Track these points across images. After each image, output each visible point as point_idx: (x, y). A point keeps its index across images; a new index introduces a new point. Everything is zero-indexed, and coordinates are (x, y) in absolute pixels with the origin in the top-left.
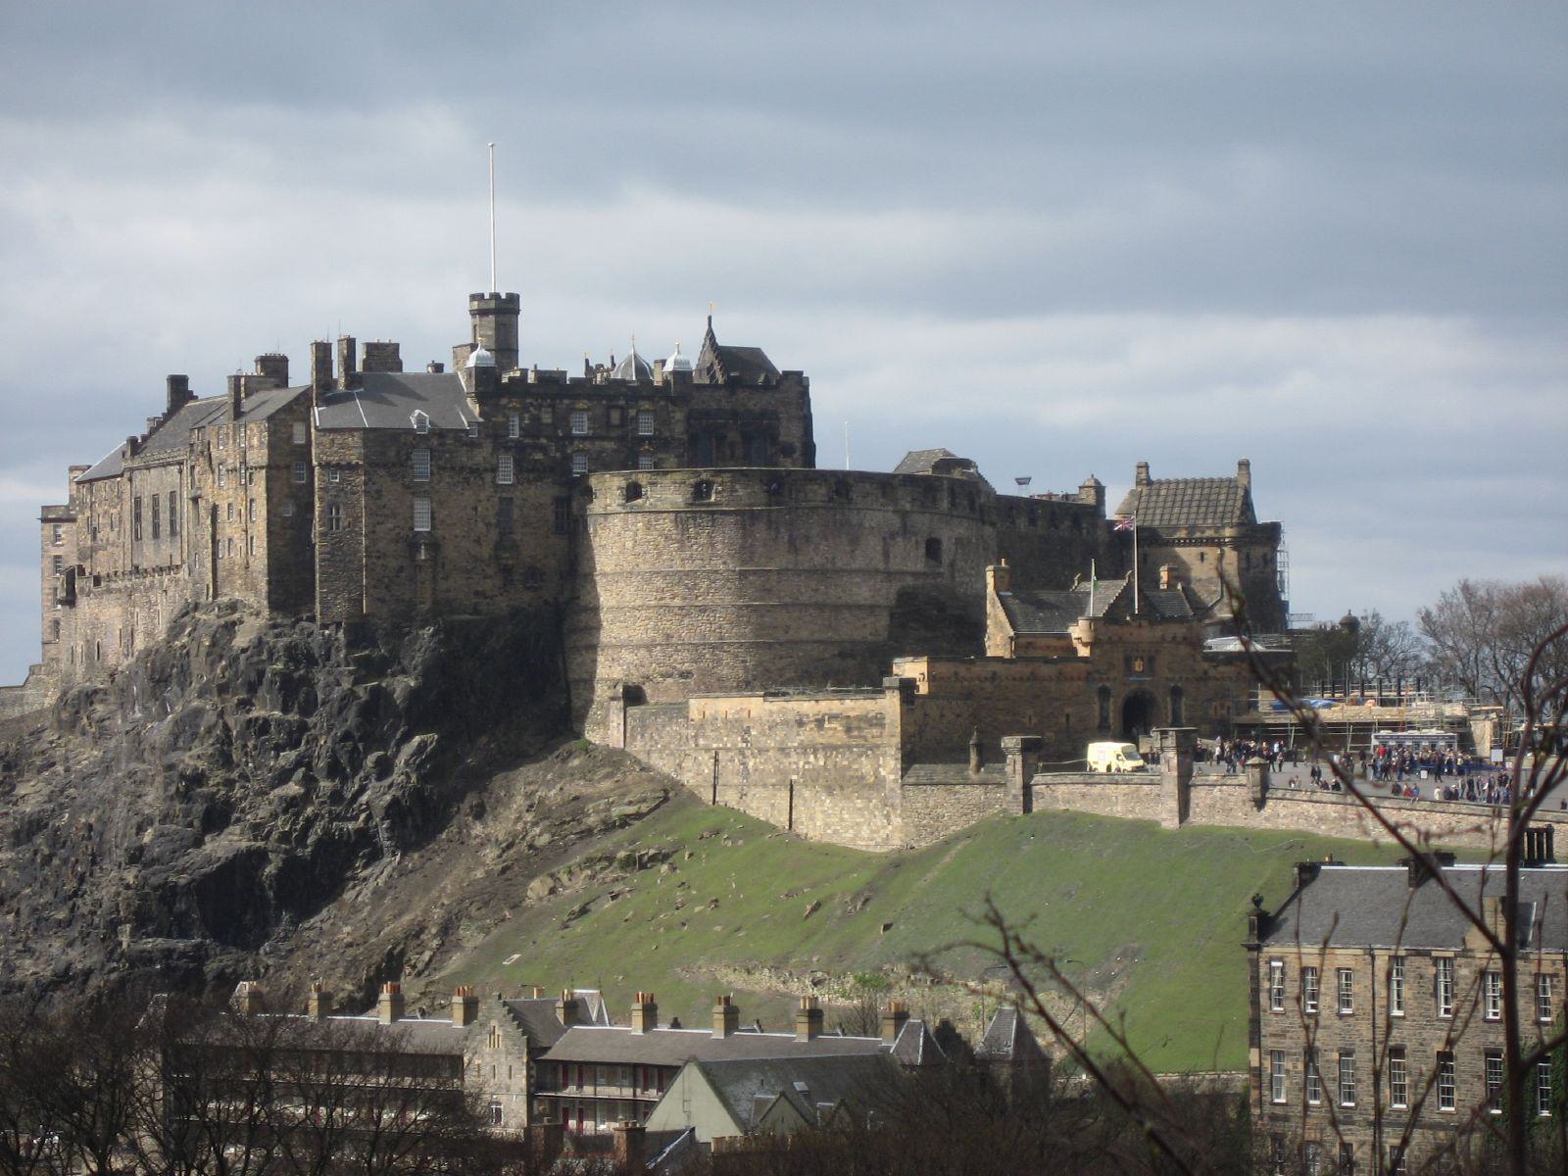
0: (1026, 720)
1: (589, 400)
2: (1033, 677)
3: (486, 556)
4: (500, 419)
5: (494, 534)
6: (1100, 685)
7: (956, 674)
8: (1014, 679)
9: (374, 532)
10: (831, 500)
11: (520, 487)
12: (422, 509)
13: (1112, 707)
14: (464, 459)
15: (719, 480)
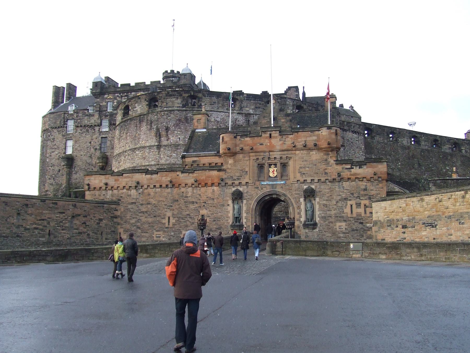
0: (166, 221)
1: (144, 91)
2: (173, 185)
3: (94, 163)
4: (104, 104)
5: (98, 154)
6: (234, 189)
7: (106, 184)
8: (155, 186)
9: (51, 156)
10: (184, 106)
11: (111, 132)
12: (70, 143)
13: (244, 208)
14: (86, 122)
15: (130, 103)
